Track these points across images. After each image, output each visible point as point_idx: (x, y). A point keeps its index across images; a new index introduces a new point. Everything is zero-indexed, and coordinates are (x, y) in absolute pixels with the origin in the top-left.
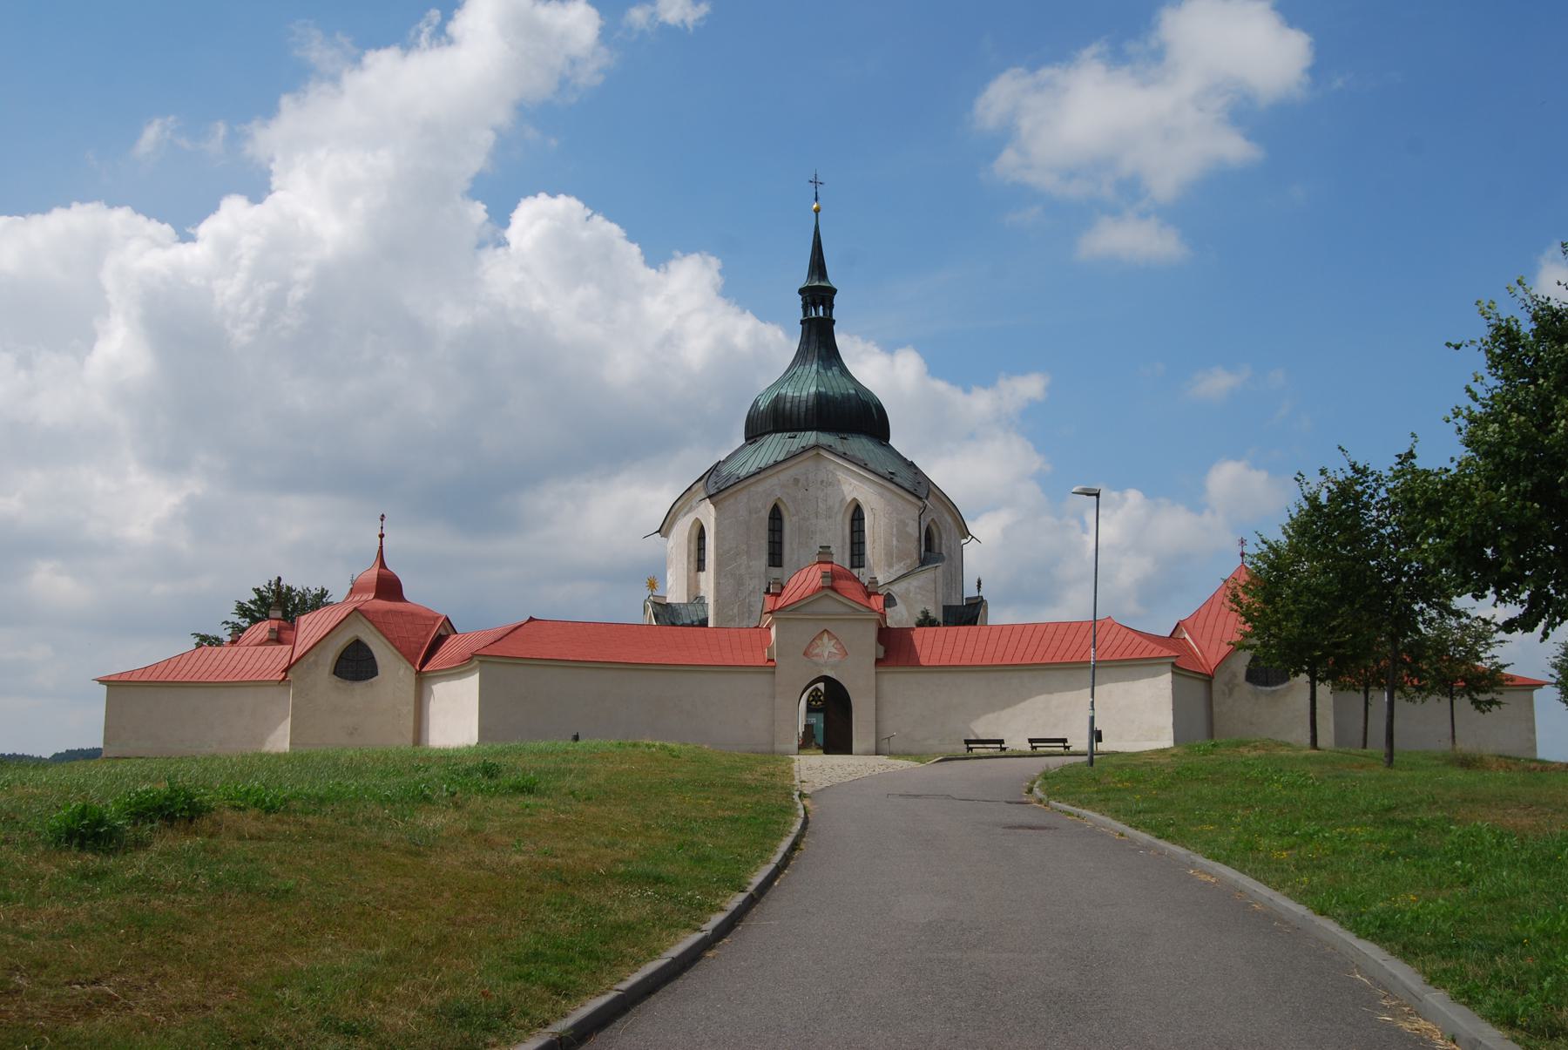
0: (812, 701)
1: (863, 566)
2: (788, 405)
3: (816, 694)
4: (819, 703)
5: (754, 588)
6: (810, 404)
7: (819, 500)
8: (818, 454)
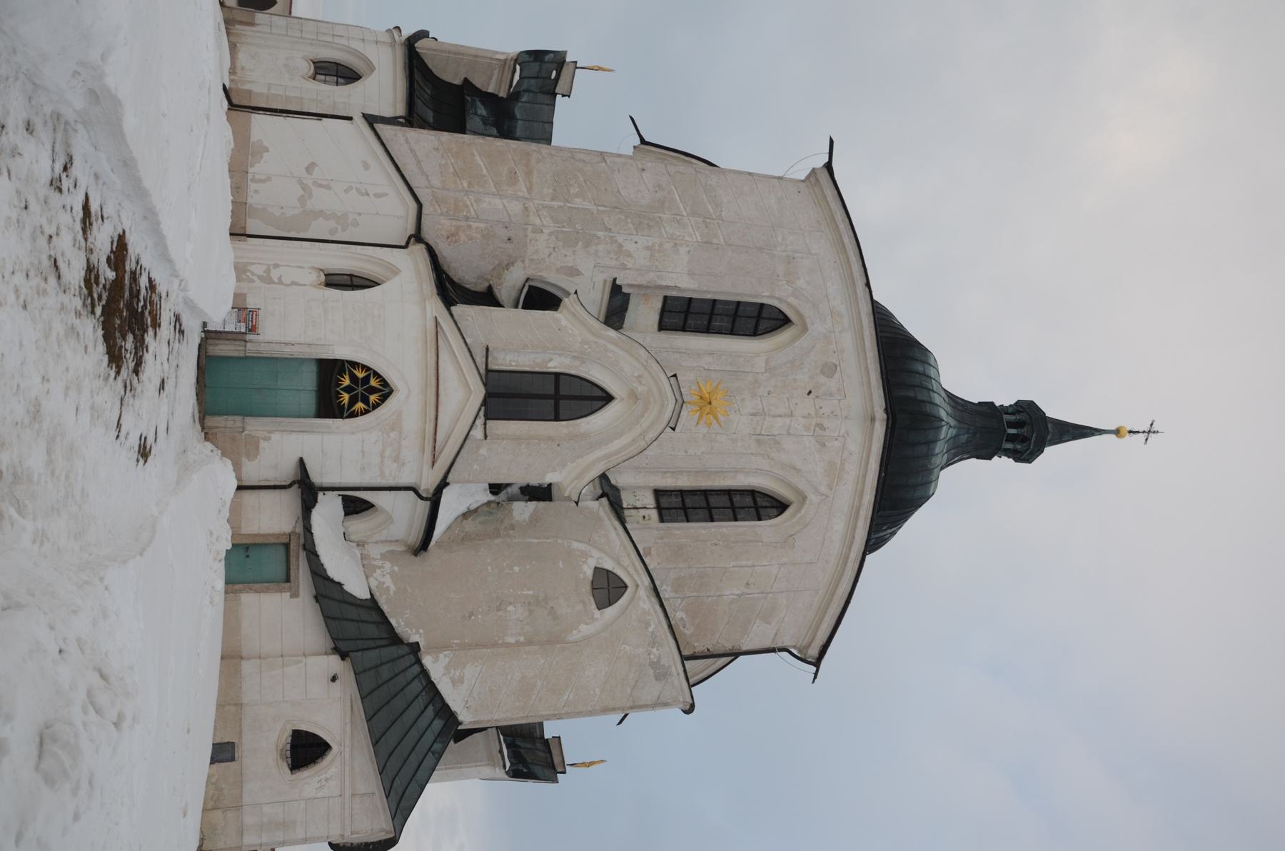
0: (354, 378)
1: (662, 520)
2: (920, 368)
3: (373, 390)
4: (346, 397)
5: (629, 255)
6: (928, 408)
7: (787, 420)
8: (873, 419)
